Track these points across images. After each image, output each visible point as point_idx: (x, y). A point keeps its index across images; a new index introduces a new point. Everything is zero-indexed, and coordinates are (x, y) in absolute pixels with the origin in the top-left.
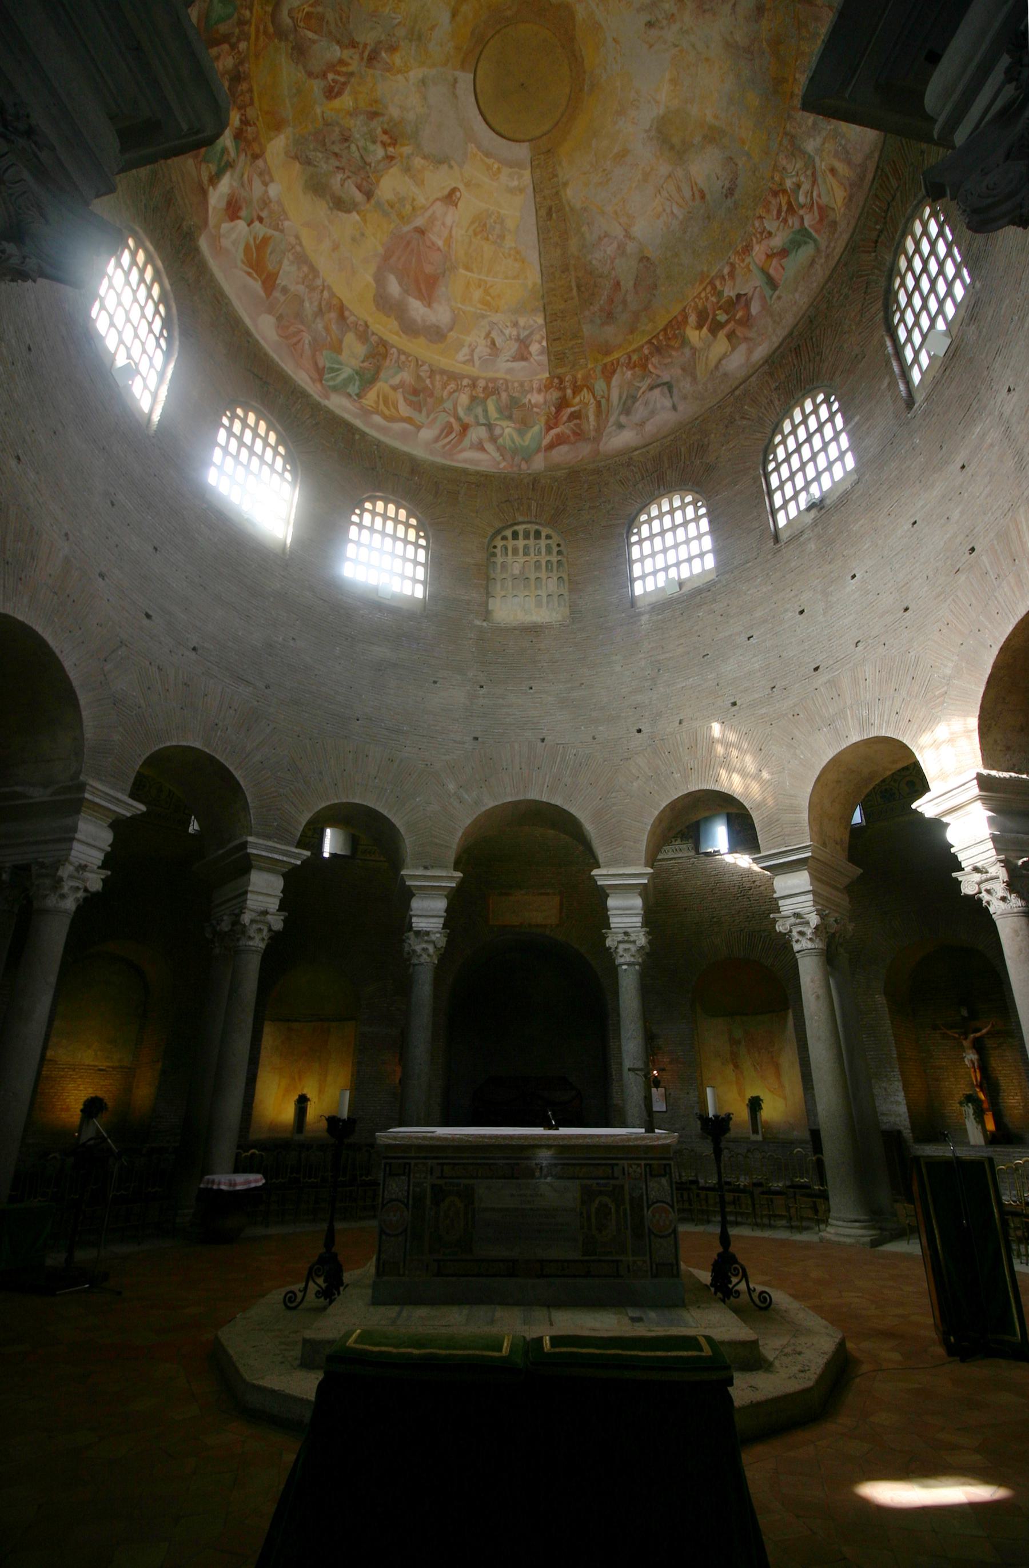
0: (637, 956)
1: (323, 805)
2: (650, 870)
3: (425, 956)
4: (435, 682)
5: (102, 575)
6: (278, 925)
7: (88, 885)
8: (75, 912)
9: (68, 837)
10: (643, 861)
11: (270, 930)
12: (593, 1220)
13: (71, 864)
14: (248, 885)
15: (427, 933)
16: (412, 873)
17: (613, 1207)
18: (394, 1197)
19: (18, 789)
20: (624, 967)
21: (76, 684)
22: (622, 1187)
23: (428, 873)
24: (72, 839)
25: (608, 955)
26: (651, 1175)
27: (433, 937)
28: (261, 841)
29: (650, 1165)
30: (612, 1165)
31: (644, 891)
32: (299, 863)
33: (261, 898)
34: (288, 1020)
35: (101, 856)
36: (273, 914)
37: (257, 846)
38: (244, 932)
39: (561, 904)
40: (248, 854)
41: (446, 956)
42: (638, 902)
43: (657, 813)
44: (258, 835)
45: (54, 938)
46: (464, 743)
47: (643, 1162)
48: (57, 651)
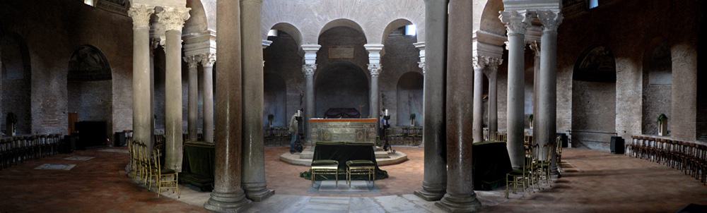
2: (383, 45)
16: (304, 46)
25: (369, 72)
31: (381, 52)
39: (354, 52)
41: (316, 72)
42: (379, 55)
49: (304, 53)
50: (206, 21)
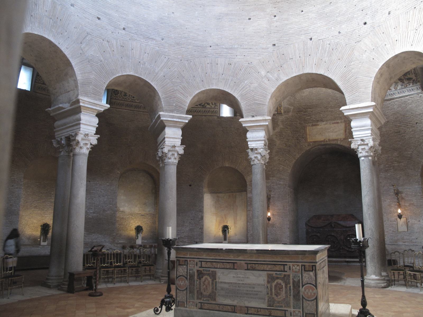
0: (370, 152)
1: (197, 92)
2: (373, 104)
3: (256, 160)
4: (250, 19)
5: (72, 5)
6: (182, 152)
7: (91, 142)
8: (89, 154)
9: (78, 123)
10: (370, 99)
11: (178, 154)
12: (273, 291)
13: (81, 134)
14: (165, 135)
15: (256, 149)
17: (284, 285)
18: (181, 274)
19: (61, 105)
20: (363, 158)
21: (69, 56)
22: (289, 275)
23: (253, 119)
24: (80, 124)
26: (305, 271)
27: (260, 151)
28: (167, 114)
29: (304, 265)
30: (284, 265)
32: (187, 121)
33: (172, 140)
34: (217, 193)
35: (95, 129)
36: (178, 147)
37: (164, 115)
38: (166, 156)
40: (162, 121)
43: (377, 70)
44: (166, 111)
45: (82, 164)
46: (268, 48)
47: (300, 264)
48: (57, 44)
49: (245, 131)
50: (76, 86)
